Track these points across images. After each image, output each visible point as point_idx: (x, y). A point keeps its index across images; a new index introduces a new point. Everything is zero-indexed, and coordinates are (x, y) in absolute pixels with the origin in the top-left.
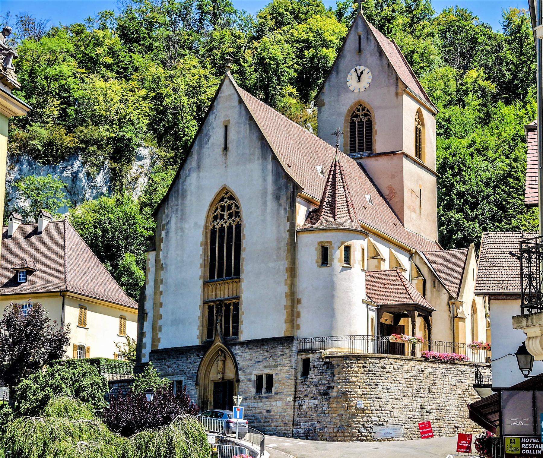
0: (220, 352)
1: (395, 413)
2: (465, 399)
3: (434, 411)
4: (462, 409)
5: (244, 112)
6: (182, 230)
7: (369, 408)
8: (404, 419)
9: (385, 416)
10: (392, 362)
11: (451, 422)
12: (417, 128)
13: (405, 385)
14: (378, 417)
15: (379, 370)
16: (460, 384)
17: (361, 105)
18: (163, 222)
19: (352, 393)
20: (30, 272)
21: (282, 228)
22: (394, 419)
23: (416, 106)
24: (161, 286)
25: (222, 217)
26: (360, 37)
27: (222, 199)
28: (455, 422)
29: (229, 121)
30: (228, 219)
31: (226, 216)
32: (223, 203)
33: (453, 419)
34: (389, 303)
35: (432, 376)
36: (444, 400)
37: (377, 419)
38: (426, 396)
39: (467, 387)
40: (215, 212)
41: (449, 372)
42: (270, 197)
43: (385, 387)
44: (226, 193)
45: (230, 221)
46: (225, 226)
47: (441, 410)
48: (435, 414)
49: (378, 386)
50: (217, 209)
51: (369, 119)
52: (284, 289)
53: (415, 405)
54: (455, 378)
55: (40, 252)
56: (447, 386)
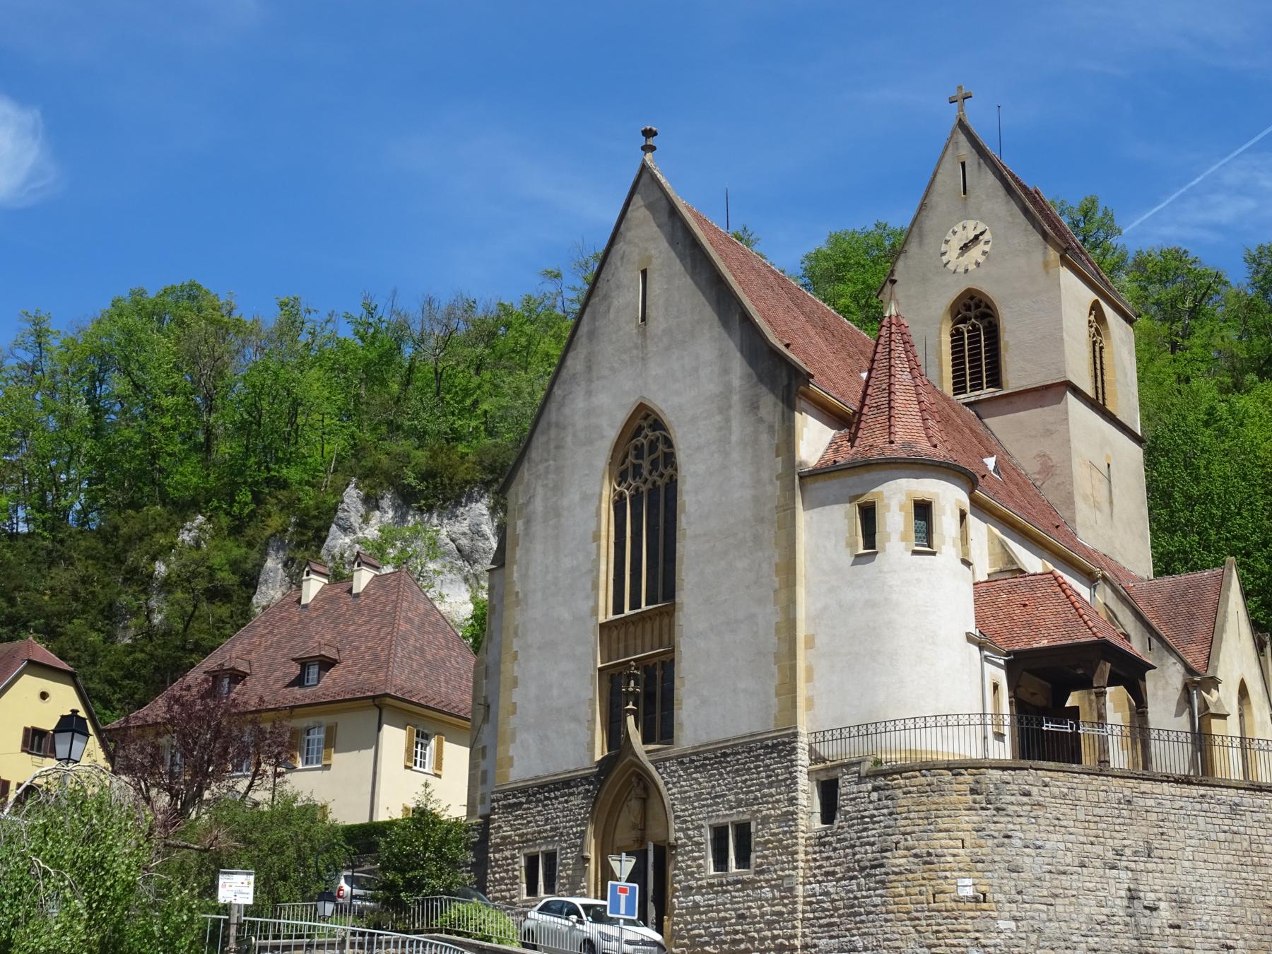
0: (634, 779)
1: (1060, 909)
2: (1244, 875)
3: (1162, 905)
4: (1237, 901)
5: (680, 234)
7: (989, 897)
8: (1084, 927)
9: (1033, 918)
10: (1047, 780)
11: (1210, 934)
12: (1094, 343)
13: (1083, 839)
14: (1015, 919)
15: (1013, 799)
16: (1229, 836)
17: (972, 298)
18: (521, 501)
19: (942, 859)
20: (326, 664)
21: (765, 475)
22: (1057, 924)
23: (1092, 296)
24: (515, 640)
25: (637, 470)
26: (963, 165)
27: (639, 431)
28: (1220, 934)
29: (650, 258)
30: (650, 473)
33: (1216, 926)
34: (1035, 646)
35: (1153, 817)
36: (1190, 878)
37: (1013, 925)
38: (1141, 866)
39: (1246, 844)
40: (623, 463)
41: (1198, 806)
43: (1029, 842)
44: (646, 417)
45: (655, 476)
46: (644, 489)
47: (1180, 904)
48: (1166, 913)
49: (1013, 841)
50: (626, 456)
51: (990, 323)
52: (769, 615)
53: (1113, 890)
54: (1215, 821)
55: (351, 629)
56: (1193, 842)
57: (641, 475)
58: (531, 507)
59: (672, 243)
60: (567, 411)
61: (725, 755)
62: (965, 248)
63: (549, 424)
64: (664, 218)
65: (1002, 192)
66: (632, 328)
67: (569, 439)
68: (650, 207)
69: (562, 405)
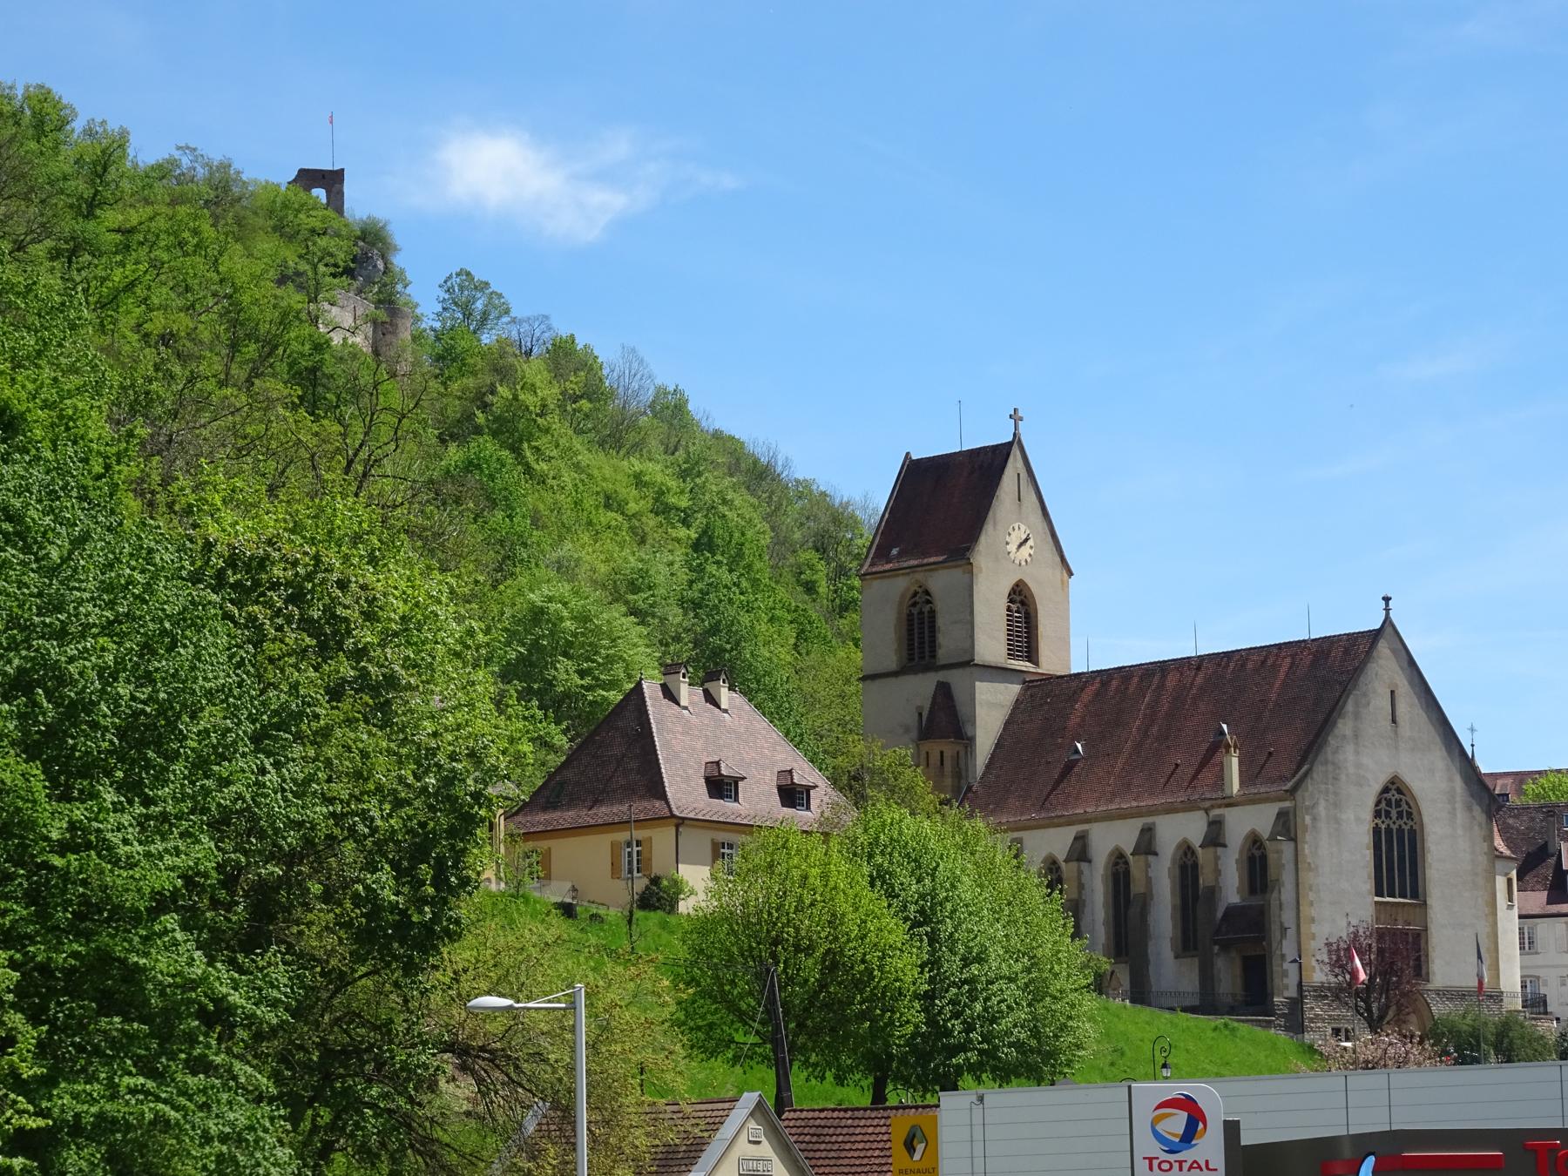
5: (1416, 680)
6: (1337, 821)
25: (1388, 815)
42: (1459, 806)
59: (1411, 683)
60: (1341, 757)
62: (1021, 545)
64: (1405, 665)
66: (1387, 723)
67: (1343, 777)
68: (1394, 651)
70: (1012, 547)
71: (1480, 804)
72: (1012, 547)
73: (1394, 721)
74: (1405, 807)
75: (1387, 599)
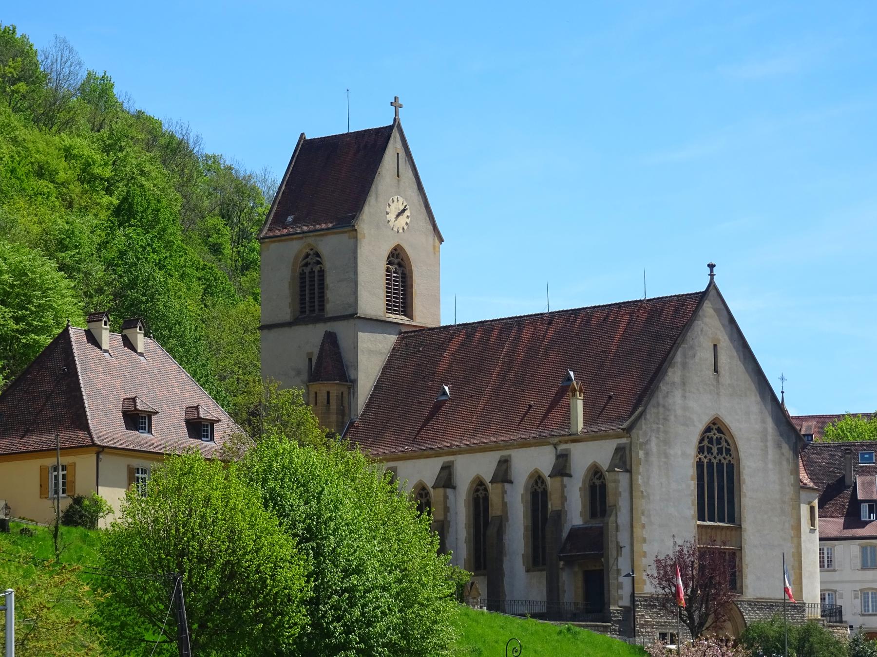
5: (736, 336)
6: (667, 456)
25: (710, 450)
31: (715, 450)
32: (710, 434)
42: (770, 444)
57: (712, 454)
58: (648, 447)
59: (731, 339)
60: (670, 401)
61: (772, 606)
63: (658, 404)
64: (726, 322)
65: (416, 187)
66: (710, 372)
67: (672, 418)
68: (717, 311)
69: (666, 396)
70: (391, 217)
71: (788, 443)
72: (391, 217)
73: (716, 371)
74: (724, 444)
75: (711, 266)
